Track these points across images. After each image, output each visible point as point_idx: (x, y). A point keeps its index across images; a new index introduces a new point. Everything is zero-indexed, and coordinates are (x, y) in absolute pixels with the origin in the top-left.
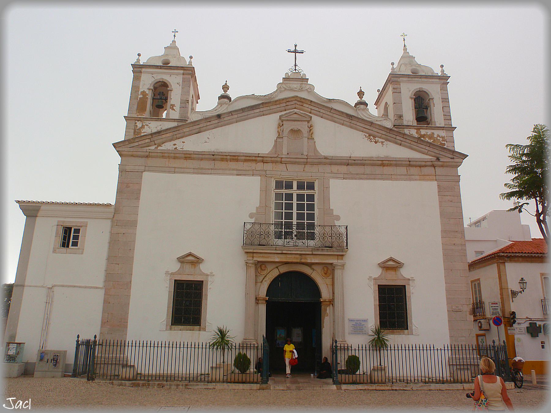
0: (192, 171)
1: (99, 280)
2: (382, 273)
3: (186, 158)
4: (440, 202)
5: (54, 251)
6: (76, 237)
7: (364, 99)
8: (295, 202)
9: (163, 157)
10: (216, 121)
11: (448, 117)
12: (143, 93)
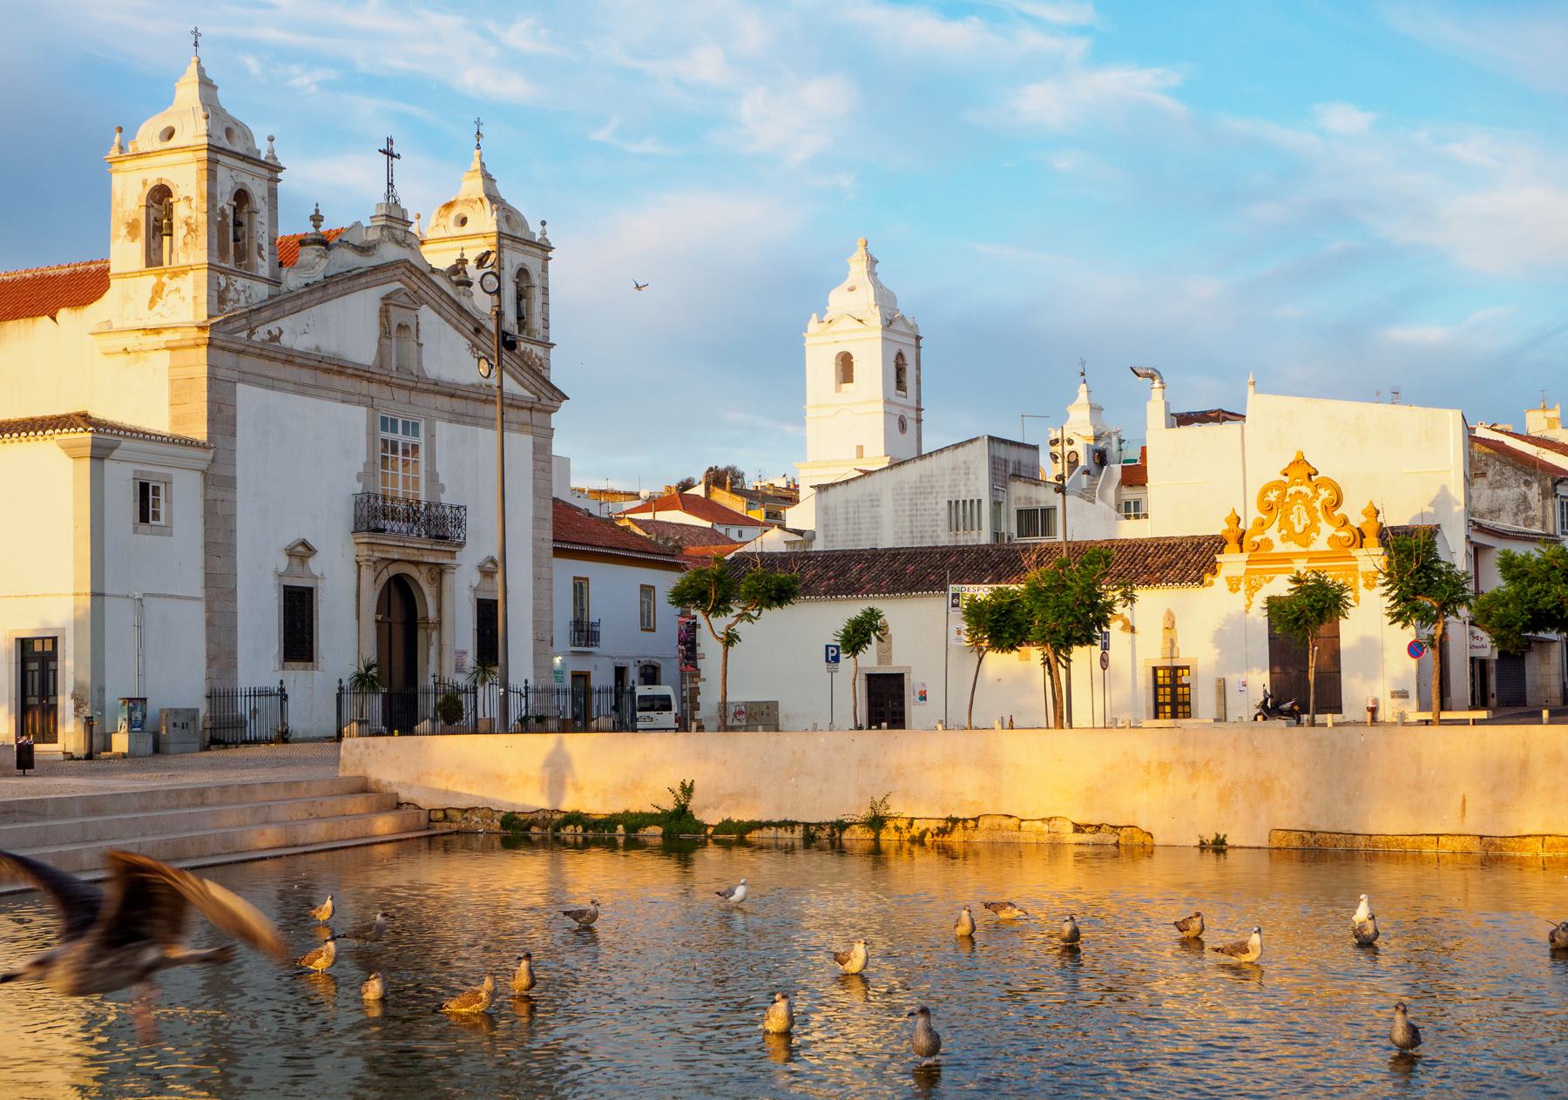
0: (291, 386)
1: (196, 587)
3: (286, 362)
5: (135, 531)
9: (260, 356)
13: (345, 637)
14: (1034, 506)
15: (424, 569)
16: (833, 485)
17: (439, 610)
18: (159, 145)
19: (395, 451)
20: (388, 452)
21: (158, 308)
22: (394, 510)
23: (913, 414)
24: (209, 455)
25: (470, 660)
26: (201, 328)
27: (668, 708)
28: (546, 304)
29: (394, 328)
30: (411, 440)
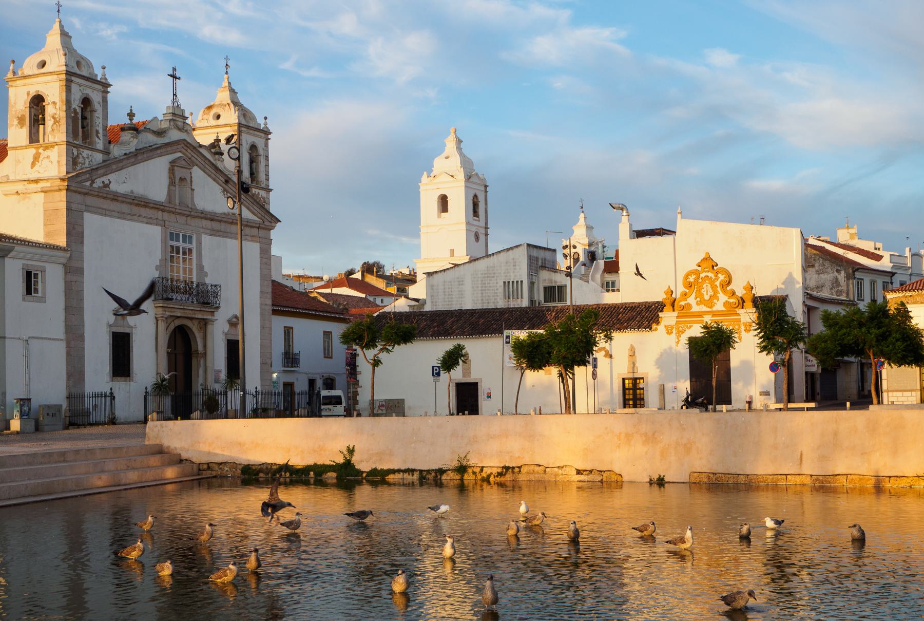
0: (116, 214)
3: (113, 200)
5: (24, 300)
9: (98, 196)
12: (75, 109)
13: (148, 361)
14: (553, 284)
15: (196, 322)
16: (436, 272)
17: (205, 346)
18: (36, 71)
19: (178, 252)
20: (173, 253)
21: (37, 167)
22: (178, 287)
23: (482, 231)
24: (68, 255)
25: (223, 375)
26: (63, 180)
27: (340, 403)
28: (267, 166)
29: (178, 180)
30: (188, 246)
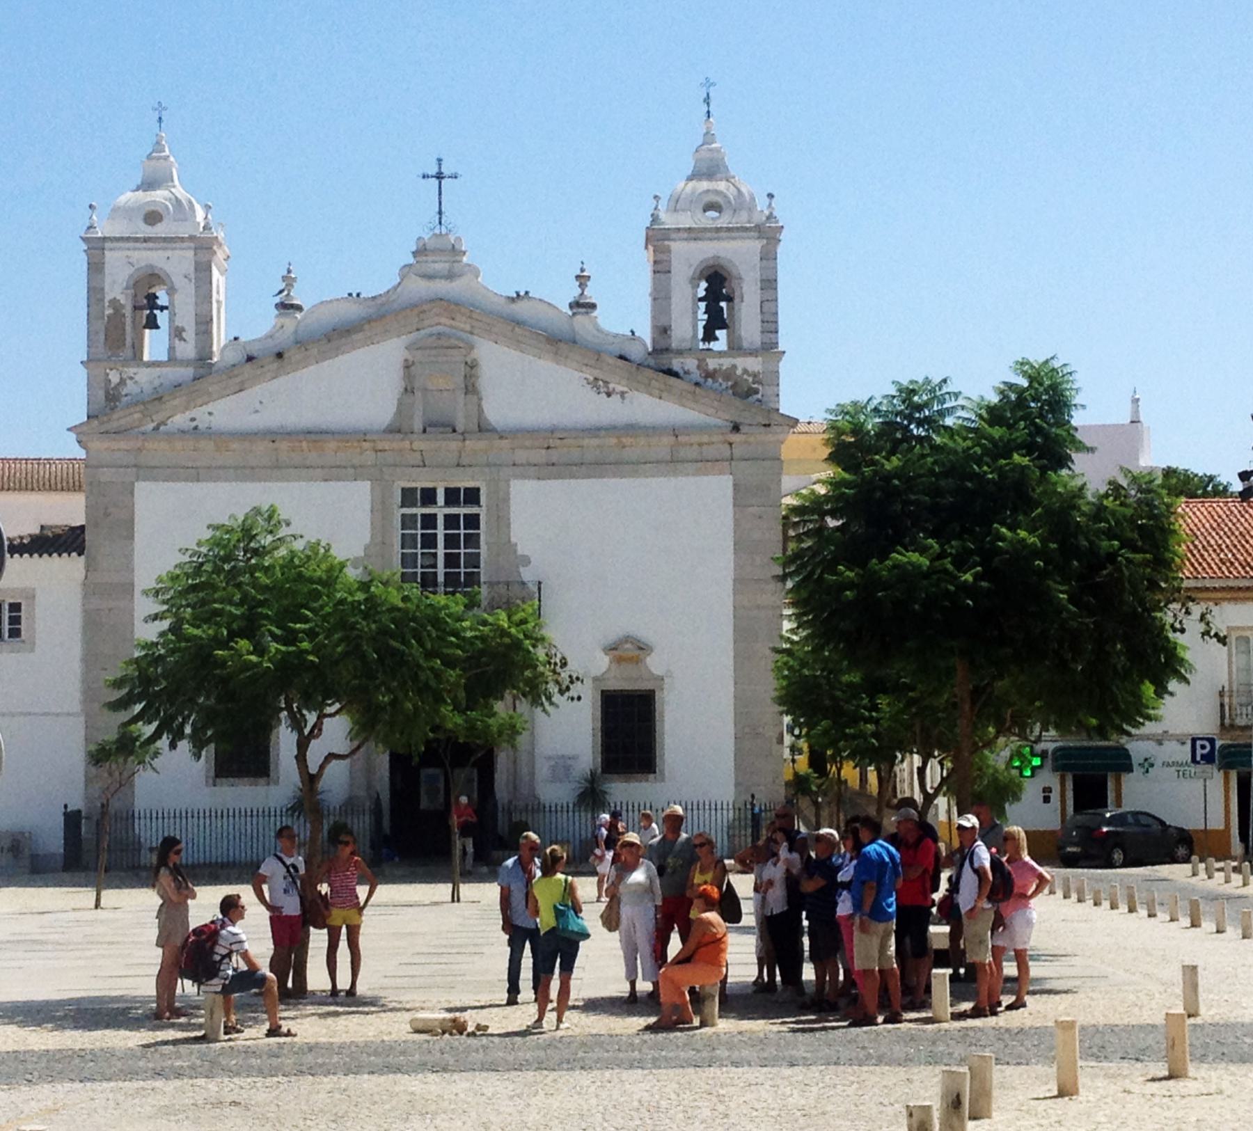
2: (609, 669)
4: (737, 523)
6: (15, 620)
7: (591, 294)
8: (441, 532)
10: (276, 365)
11: (770, 325)
12: (114, 303)
